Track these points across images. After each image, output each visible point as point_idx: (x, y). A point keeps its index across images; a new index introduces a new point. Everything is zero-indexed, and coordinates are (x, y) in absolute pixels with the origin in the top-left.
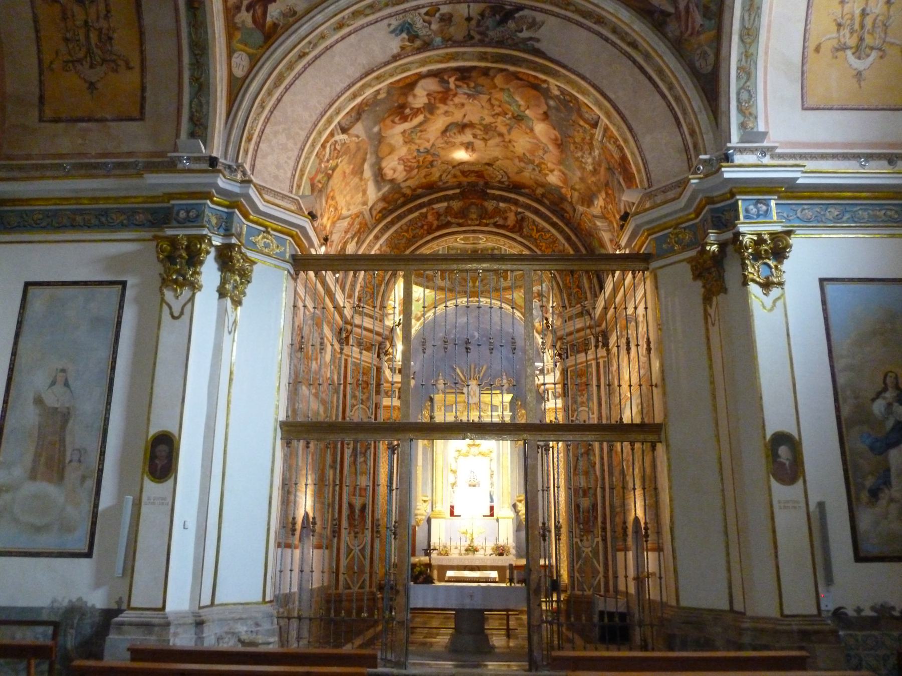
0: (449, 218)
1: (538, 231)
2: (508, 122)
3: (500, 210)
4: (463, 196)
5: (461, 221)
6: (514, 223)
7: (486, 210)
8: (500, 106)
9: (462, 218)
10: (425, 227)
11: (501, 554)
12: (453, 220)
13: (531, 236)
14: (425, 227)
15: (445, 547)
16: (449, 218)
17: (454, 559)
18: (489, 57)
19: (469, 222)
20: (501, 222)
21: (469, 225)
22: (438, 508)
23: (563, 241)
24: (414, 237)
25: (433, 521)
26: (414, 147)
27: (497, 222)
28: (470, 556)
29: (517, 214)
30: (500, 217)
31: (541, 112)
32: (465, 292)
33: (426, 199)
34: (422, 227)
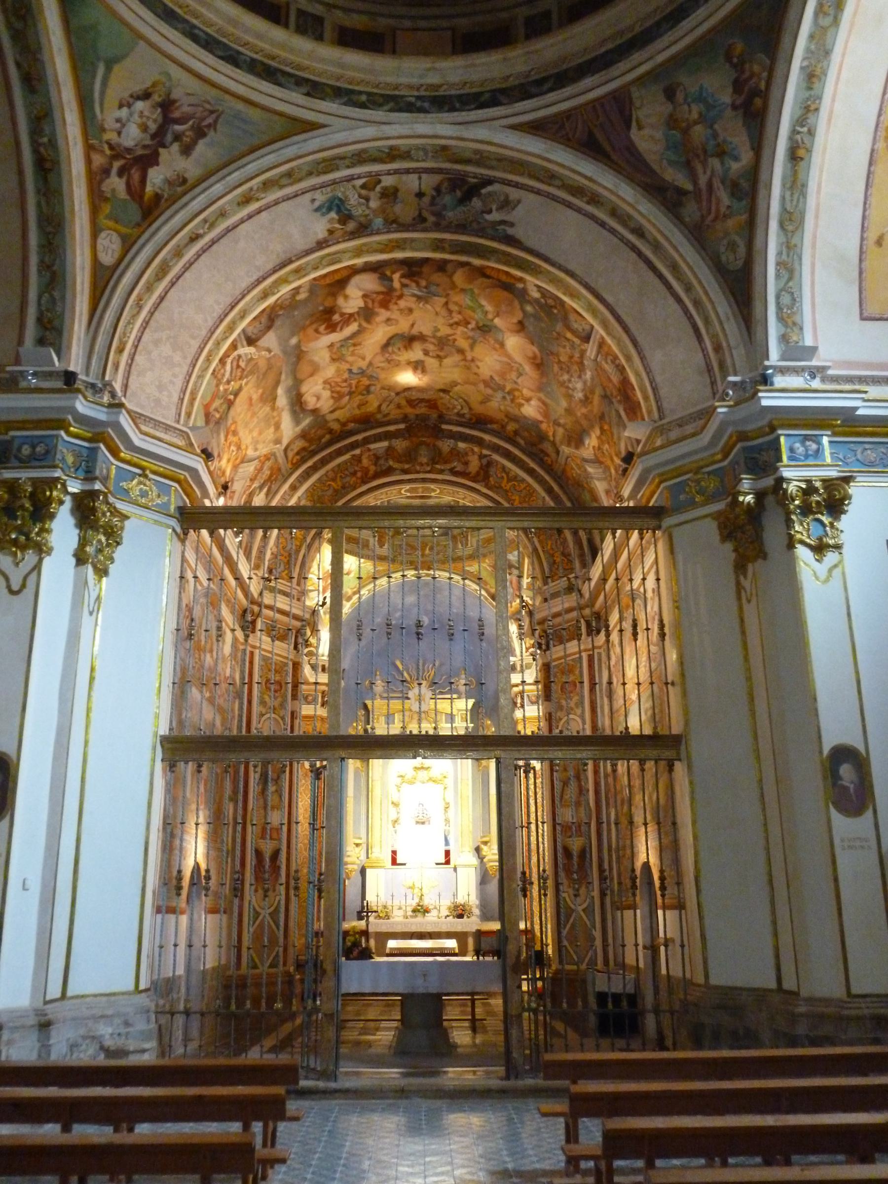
0: (391, 463)
1: (509, 480)
2: (471, 334)
4: (409, 432)
5: (406, 466)
7: (439, 452)
8: (460, 313)
9: (407, 462)
10: (359, 474)
11: (460, 916)
12: (396, 465)
14: (359, 474)
15: (385, 907)
16: (391, 463)
17: (397, 923)
18: (447, 246)
19: (418, 468)
20: (459, 468)
21: (418, 472)
22: (375, 854)
23: (543, 494)
24: (343, 487)
25: (369, 873)
26: (345, 366)
28: (420, 919)
29: (481, 457)
30: (459, 461)
31: (515, 320)
32: (411, 563)
33: (359, 437)
34: (354, 474)
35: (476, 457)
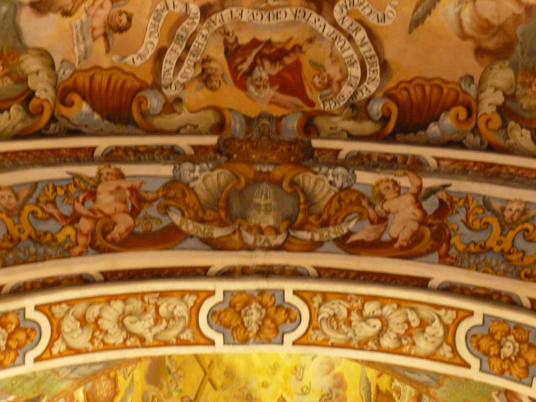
0: (176, 218)
3: (361, 196)
5: (218, 233)
6: (414, 226)
7: (310, 200)
9: (222, 224)
10: (85, 225)
12: (189, 227)
13: (484, 248)
14: (85, 225)
19: (250, 239)
27: (350, 233)
35: (408, 199)
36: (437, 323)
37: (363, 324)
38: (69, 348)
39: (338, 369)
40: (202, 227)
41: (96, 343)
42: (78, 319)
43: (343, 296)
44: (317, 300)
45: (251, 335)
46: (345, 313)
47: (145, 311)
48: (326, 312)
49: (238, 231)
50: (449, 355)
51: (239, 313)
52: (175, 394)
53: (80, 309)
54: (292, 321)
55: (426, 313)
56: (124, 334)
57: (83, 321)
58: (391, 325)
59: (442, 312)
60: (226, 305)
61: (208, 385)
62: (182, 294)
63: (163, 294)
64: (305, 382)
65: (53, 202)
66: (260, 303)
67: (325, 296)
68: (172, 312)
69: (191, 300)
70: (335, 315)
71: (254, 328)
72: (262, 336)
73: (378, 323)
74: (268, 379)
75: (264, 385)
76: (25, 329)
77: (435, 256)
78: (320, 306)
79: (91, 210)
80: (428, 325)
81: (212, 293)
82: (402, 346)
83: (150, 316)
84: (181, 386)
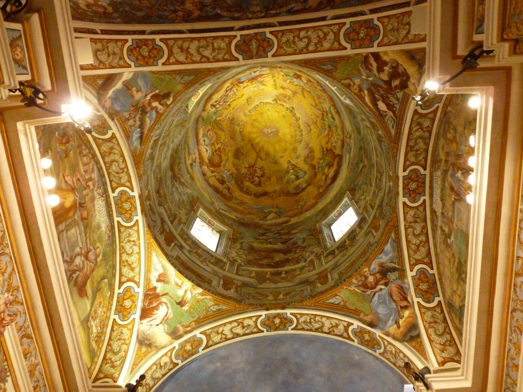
0: (219, 11)
5: (236, 15)
9: (238, 12)
10: (180, 13)
12: (225, 14)
14: (180, 13)
21: (250, 19)
27: (292, 8)
34: (175, 11)
36: (331, 33)
37: (300, 42)
38: (177, 61)
39: (310, 145)
40: (230, 13)
41: (189, 60)
42: (179, 48)
43: (290, 31)
44: (280, 34)
45: (254, 54)
46: (292, 38)
47: (208, 46)
48: (284, 39)
49: (245, 13)
50: (337, 46)
51: (248, 45)
52: (246, 163)
53: (180, 43)
54: (271, 46)
55: (326, 30)
56: (200, 56)
57: (181, 49)
58: (312, 40)
59: (332, 27)
60: (242, 42)
61: (259, 159)
62: (223, 37)
63: (215, 38)
64: (298, 153)
65: (166, 6)
66: (256, 39)
67: (283, 32)
68: (219, 46)
69: (227, 40)
70: (288, 40)
71: (255, 51)
72: (259, 54)
73: (306, 40)
74: (283, 155)
75: (282, 157)
76: (156, 49)
77: (328, 8)
78: (281, 37)
79: (182, 9)
80: (328, 35)
81: (235, 37)
82: (317, 48)
83: (210, 48)
84: (248, 160)
